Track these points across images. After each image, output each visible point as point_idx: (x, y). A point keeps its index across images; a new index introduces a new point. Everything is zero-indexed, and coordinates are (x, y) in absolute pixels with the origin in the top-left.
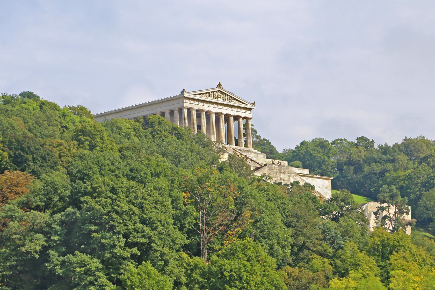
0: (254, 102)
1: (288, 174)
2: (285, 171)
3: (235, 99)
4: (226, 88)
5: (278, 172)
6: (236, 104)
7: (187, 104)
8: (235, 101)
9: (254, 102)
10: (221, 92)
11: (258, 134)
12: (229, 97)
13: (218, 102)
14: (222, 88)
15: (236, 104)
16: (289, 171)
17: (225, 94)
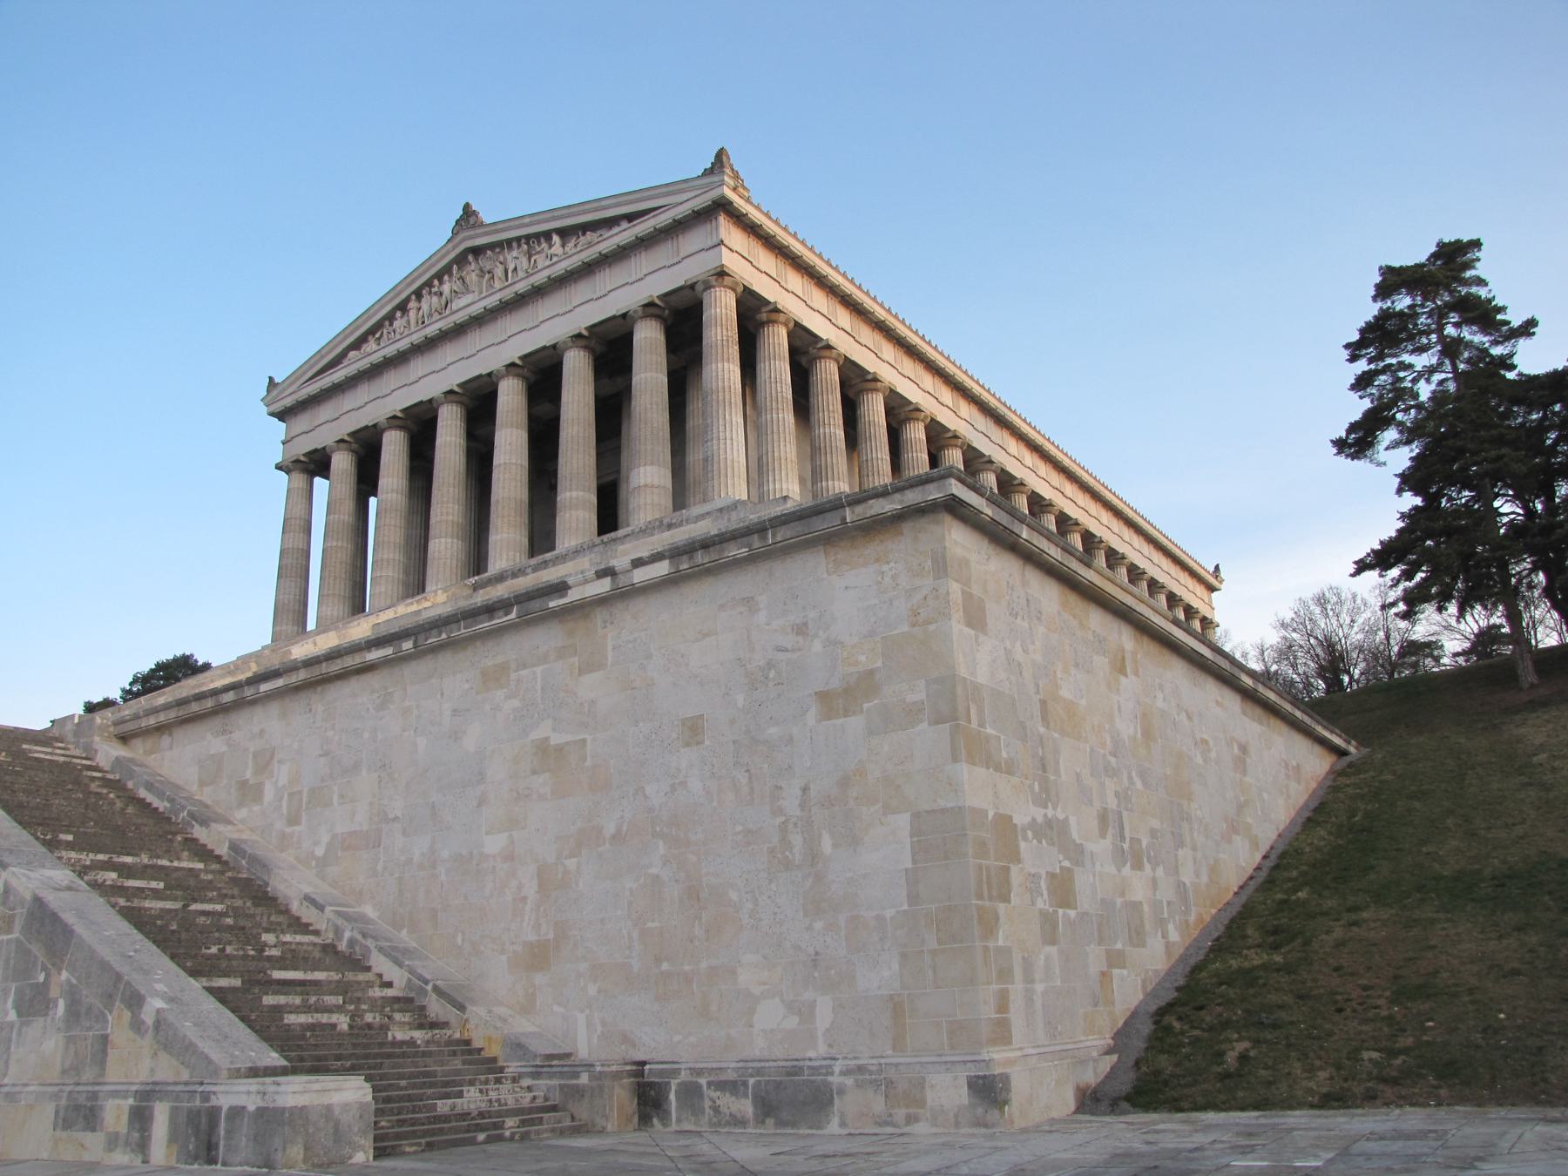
3: (564, 233)
10: (477, 251)
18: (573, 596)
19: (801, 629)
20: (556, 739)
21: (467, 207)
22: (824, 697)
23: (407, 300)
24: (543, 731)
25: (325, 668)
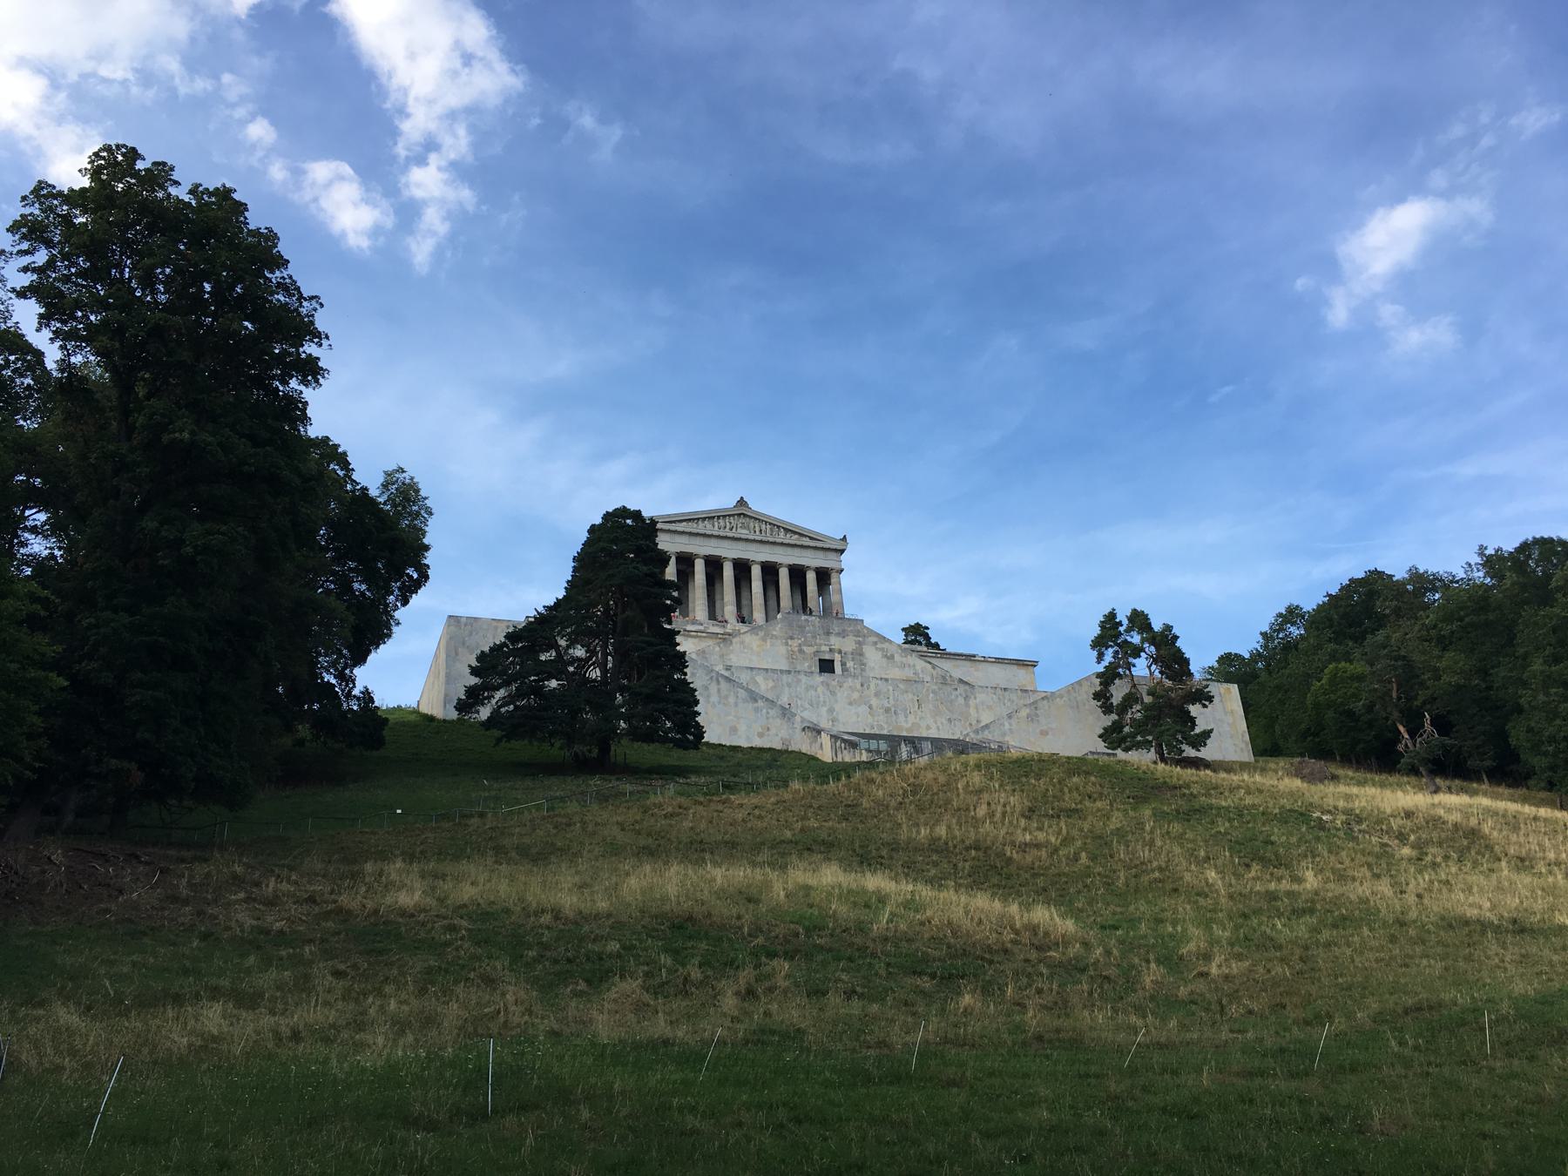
0: (845, 536)
1: (855, 638)
2: (844, 631)
4: (756, 505)
5: (821, 632)
6: (794, 539)
9: (845, 536)
11: (933, 641)
12: (768, 526)
13: (739, 536)
15: (794, 539)
17: (759, 520)
21: (742, 498)
23: (714, 517)
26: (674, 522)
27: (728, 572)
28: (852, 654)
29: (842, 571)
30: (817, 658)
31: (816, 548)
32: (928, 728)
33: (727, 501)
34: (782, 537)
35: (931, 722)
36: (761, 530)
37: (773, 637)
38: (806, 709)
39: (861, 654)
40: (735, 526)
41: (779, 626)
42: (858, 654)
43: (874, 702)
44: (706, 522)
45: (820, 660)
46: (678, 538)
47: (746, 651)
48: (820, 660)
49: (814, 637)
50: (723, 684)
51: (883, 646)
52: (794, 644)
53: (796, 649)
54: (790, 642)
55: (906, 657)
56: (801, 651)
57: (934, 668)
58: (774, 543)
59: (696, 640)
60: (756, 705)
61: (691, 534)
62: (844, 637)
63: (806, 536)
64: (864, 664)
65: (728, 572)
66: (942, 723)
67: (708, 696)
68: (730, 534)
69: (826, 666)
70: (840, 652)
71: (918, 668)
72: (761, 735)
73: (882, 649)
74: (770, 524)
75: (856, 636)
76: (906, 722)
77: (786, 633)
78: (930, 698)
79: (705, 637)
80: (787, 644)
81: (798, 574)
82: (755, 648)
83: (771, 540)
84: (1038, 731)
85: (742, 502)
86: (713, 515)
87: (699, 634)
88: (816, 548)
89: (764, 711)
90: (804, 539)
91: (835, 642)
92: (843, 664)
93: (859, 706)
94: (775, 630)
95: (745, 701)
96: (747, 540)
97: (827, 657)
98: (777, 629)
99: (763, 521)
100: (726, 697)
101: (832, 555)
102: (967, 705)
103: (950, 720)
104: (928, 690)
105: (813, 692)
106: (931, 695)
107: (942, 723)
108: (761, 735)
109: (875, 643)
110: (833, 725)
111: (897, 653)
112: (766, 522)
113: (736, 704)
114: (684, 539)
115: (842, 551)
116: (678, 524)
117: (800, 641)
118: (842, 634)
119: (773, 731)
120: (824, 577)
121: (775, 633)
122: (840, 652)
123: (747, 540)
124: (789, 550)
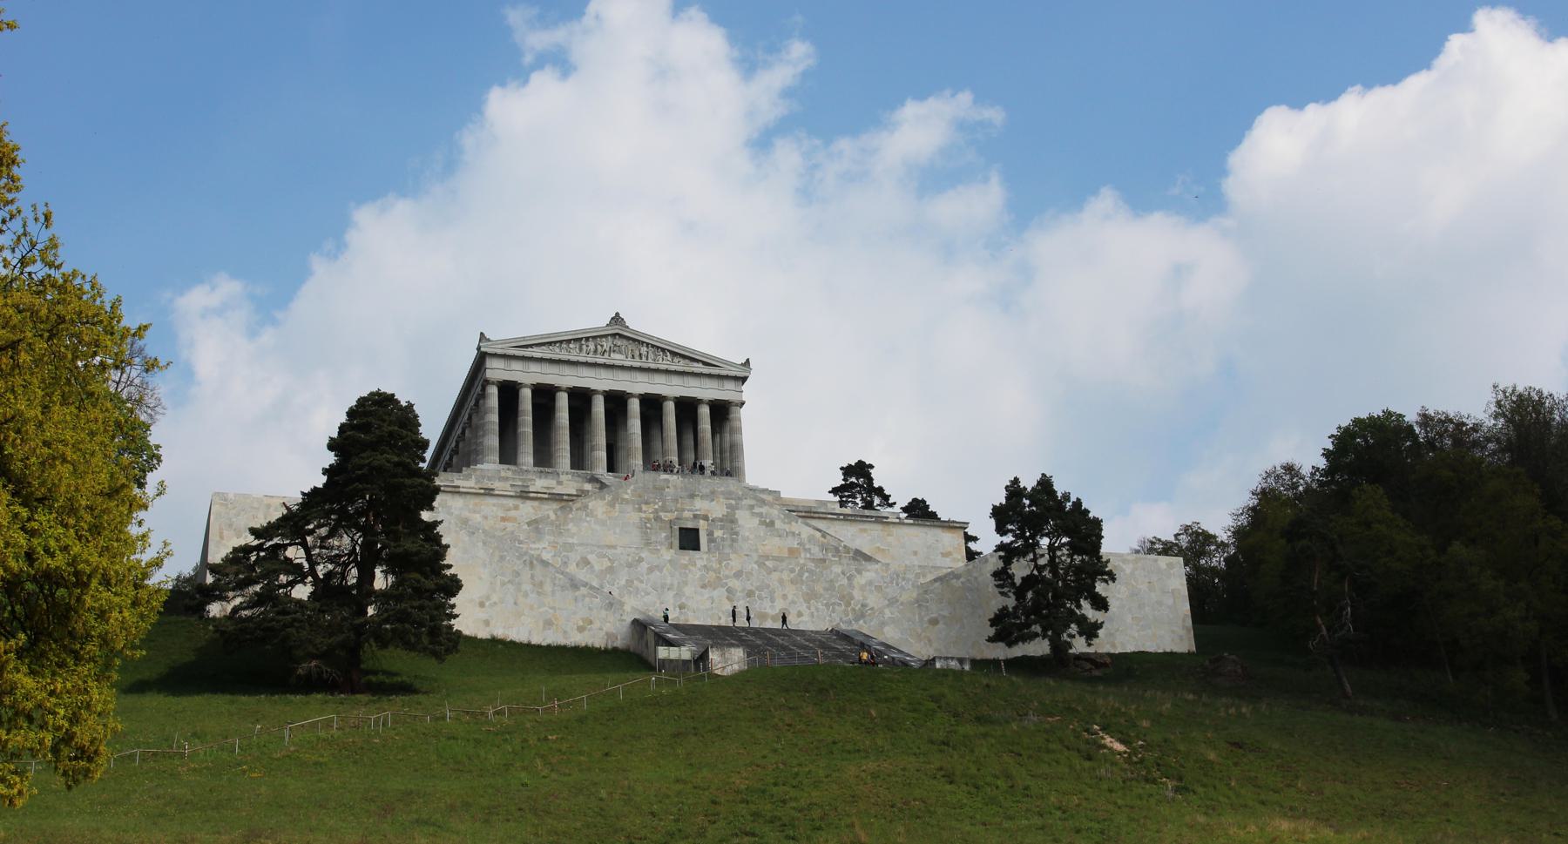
0: (748, 360)
1: (725, 501)
3: (674, 354)
4: (637, 323)
5: (684, 494)
6: (680, 365)
7: (497, 371)
8: (676, 360)
9: (748, 360)
10: (621, 336)
11: (876, 485)
13: (611, 362)
14: (627, 327)
15: (680, 365)
16: (730, 493)
17: (638, 341)
18: (889, 520)
19: (937, 541)
20: (882, 547)
21: (617, 314)
22: (942, 553)
23: (582, 338)
24: (878, 545)
25: (812, 515)
26: (531, 346)
27: (599, 407)
28: (721, 520)
29: (743, 404)
30: (677, 527)
31: (710, 376)
32: (800, 614)
33: (599, 320)
34: (665, 363)
35: (803, 608)
36: (640, 354)
37: (627, 502)
38: (648, 594)
39: (733, 521)
40: (608, 349)
41: (632, 487)
42: (729, 521)
43: (735, 584)
44: (571, 346)
45: (681, 529)
46: (534, 367)
47: (588, 519)
48: (681, 529)
49: (676, 501)
50: (539, 569)
51: (761, 510)
52: (649, 510)
53: (652, 516)
54: (644, 507)
55: (789, 523)
56: (657, 518)
57: (824, 536)
58: (657, 371)
59: (536, 503)
60: (577, 593)
61: (551, 361)
62: (713, 500)
63: (697, 361)
64: (737, 534)
65: (599, 407)
66: (817, 609)
67: (520, 584)
68: (601, 360)
69: (689, 539)
70: (706, 518)
71: (804, 536)
72: (581, 629)
73: (760, 515)
74: (653, 346)
75: (727, 499)
76: (772, 607)
77: (640, 496)
78: (804, 578)
79: (546, 499)
80: (640, 510)
81: (687, 408)
82: (600, 516)
83: (653, 366)
84: (926, 619)
85: (617, 319)
86: (580, 336)
87: (539, 495)
88: (710, 376)
89: (587, 599)
90: (695, 364)
91: (700, 505)
92: (710, 534)
93: (714, 589)
94: (627, 494)
95: (563, 588)
96: (622, 368)
97: (690, 525)
98: (629, 491)
99: (643, 342)
100: (541, 584)
101: (730, 385)
102: (851, 586)
103: (827, 605)
104: (802, 568)
105: (658, 573)
106: (806, 574)
107: (817, 609)
108: (581, 629)
109: (752, 507)
110: (681, 613)
111: (779, 518)
112: (648, 344)
113: (553, 592)
114: (547, 368)
115: (744, 379)
116: (535, 349)
117: (656, 507)
118: (712, 496)
119: (597, 624)
120: (722, 412)
121: (626, 496)
122: (706, 518)
123: (622, 368)
124: (676, 380)
